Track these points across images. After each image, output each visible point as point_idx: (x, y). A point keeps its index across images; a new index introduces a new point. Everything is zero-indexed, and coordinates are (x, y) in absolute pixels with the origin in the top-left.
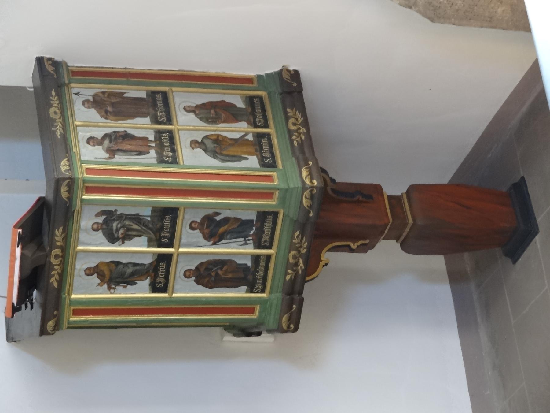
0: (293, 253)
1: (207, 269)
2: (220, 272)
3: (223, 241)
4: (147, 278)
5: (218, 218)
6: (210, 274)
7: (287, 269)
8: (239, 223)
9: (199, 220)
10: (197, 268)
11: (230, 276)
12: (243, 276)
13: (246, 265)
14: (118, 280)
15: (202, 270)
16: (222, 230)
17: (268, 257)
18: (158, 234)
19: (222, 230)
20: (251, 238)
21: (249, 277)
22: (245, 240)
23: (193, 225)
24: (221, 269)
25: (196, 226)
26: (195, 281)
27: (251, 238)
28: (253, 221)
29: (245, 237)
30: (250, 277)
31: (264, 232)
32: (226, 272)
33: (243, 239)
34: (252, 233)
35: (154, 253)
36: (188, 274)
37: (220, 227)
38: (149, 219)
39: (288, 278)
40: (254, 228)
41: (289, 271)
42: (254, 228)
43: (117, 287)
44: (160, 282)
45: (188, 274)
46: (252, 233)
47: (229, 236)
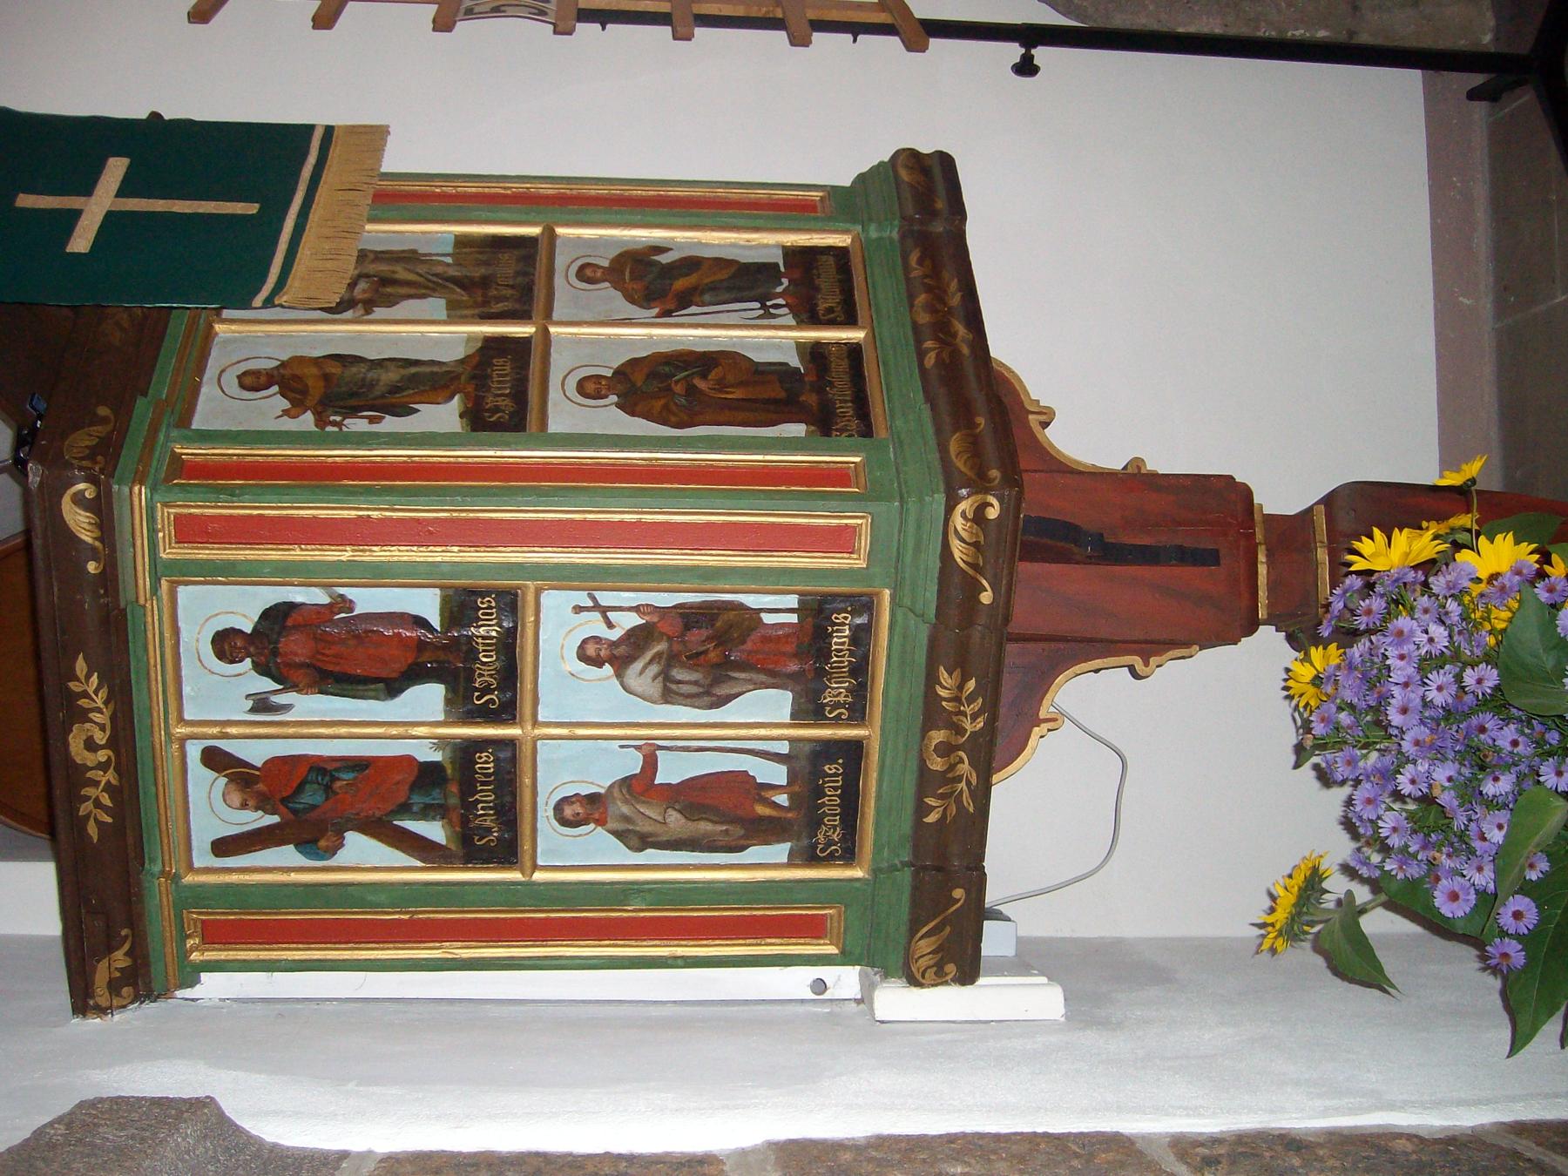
0: (922, 298)
1: (653, 375)
2: (701, 384)
3: (693, 309)
4: (451, 397)
5: (664, 259)
6: (669, 389)
7: (919, 342)
8: (733, 270)
9: (606, 264)
10: (619, 372)
11: (737, 394)
12: (783, 395)
13: (786, 364)
14: (353, 402)
15: (639, 378)
16: (680, 284)
17: (854, 351)
18: (479, 293)
19: (680, 284)
20: (781, 301)
21: (802, 398)
22: (763, 306)
23: (588, 272)
24: (704, 376)
25: (599, 275)
26: (618, 406)
27: (781, 301)
28: (777, 265)
29: (762, 300)
30: (811, 399)
31: (817, 289)
32: (722, 385)
33: (757, 305)
34: (779, 289)
35: (470, 338)
36: (590, 387)
37: (676, 278)
38: (449, 260)
39: (930, 360)
40: (785, 281)
41: (929, 344)
42: (785, 281)
43: (347, 421)
44: (497, 409)
45: (590, 387)
46: (779, 289)
47: (707, 297)
